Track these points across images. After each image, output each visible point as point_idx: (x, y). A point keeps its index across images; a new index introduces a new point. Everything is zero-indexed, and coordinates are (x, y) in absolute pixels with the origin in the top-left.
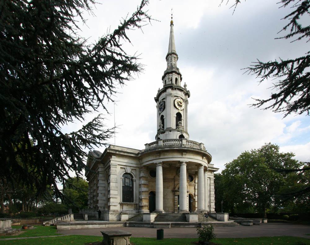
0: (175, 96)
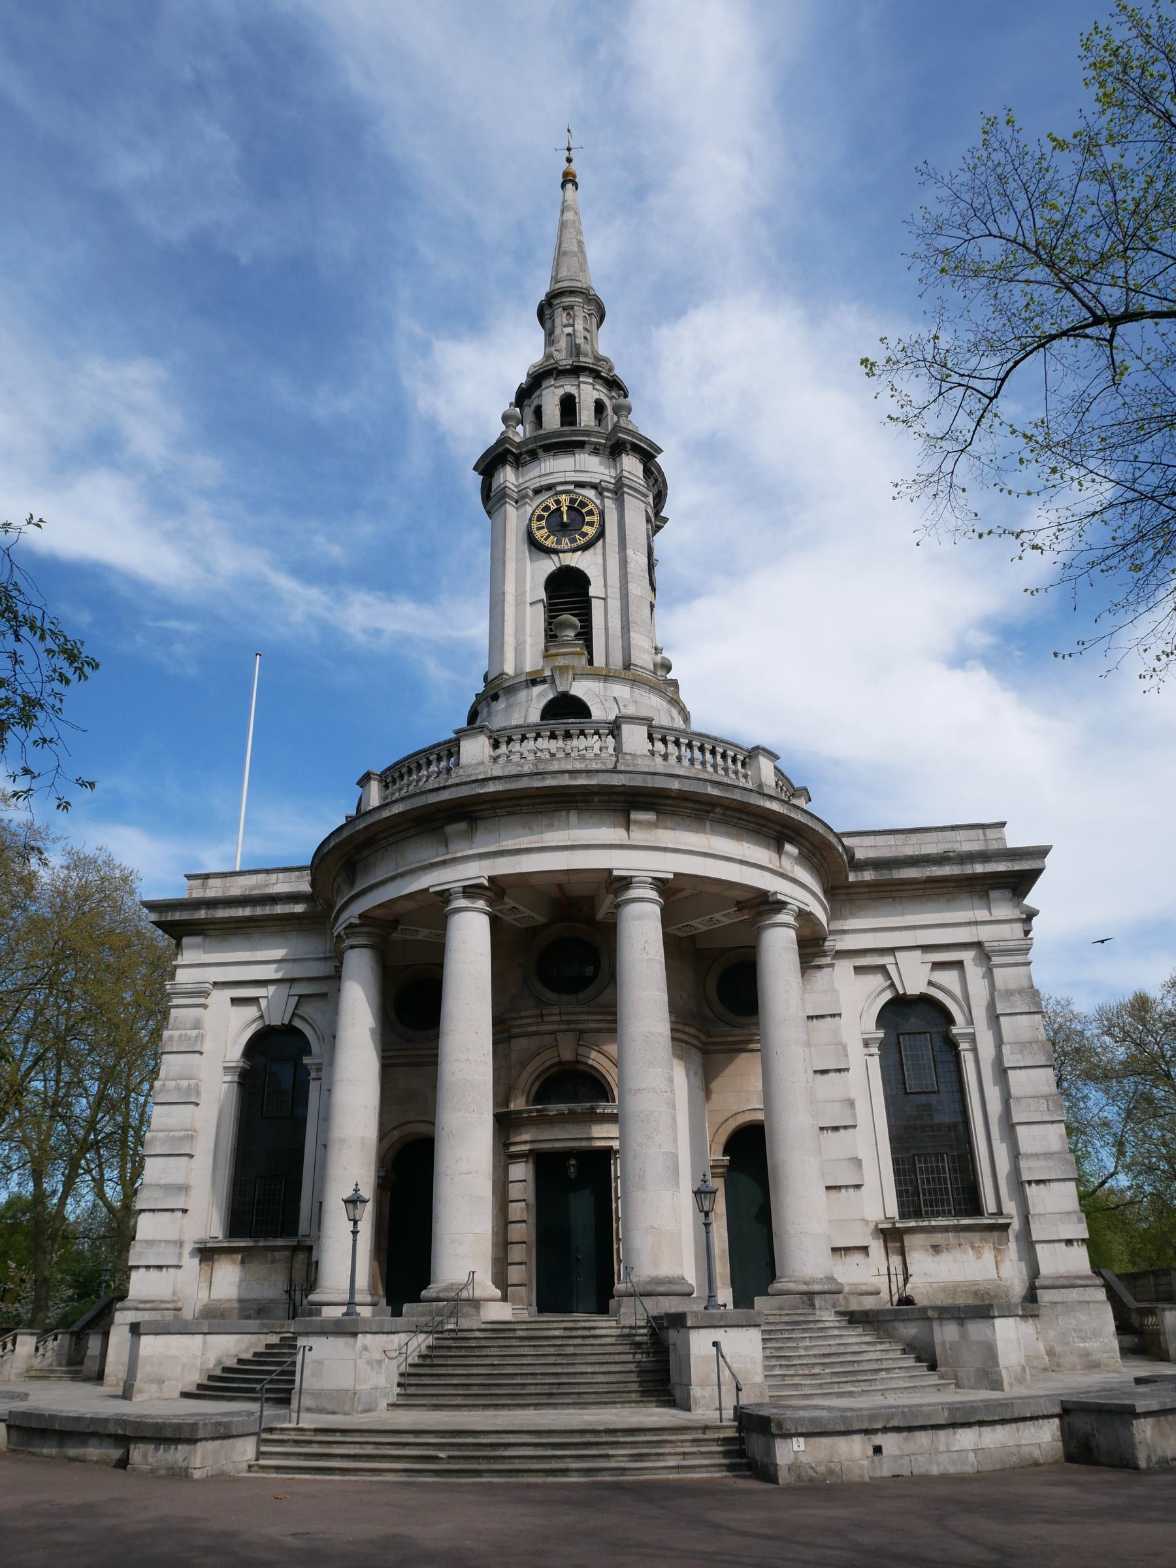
0: (537, 492)
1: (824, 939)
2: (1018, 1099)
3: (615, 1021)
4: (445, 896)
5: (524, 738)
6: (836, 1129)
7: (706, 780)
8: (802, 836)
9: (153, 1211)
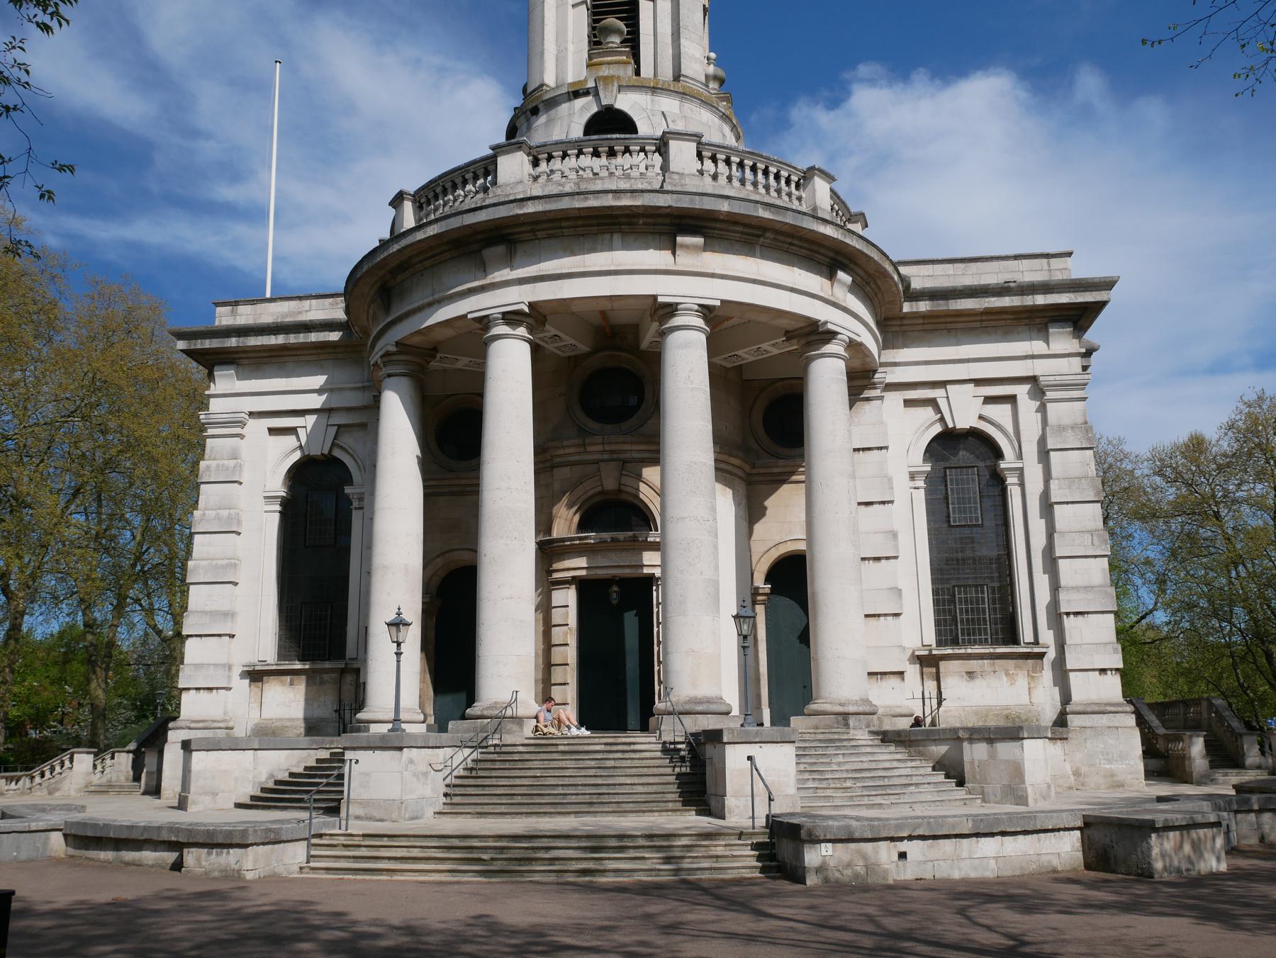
1: (875, 371)
2: (1063, 533)
3: (658, 451)
4: (484, 322)
5: (565, 156)
6: (878, 559)
7: (757, 202)
8: (856, 264)
9: (200, 636)
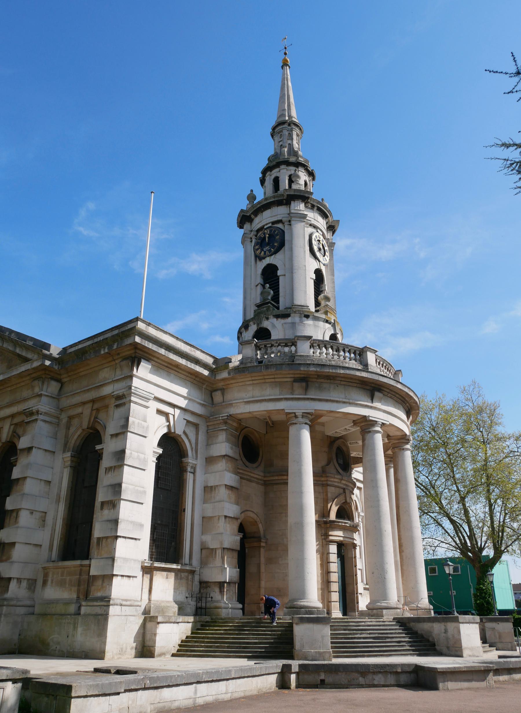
9: (125, 537)
